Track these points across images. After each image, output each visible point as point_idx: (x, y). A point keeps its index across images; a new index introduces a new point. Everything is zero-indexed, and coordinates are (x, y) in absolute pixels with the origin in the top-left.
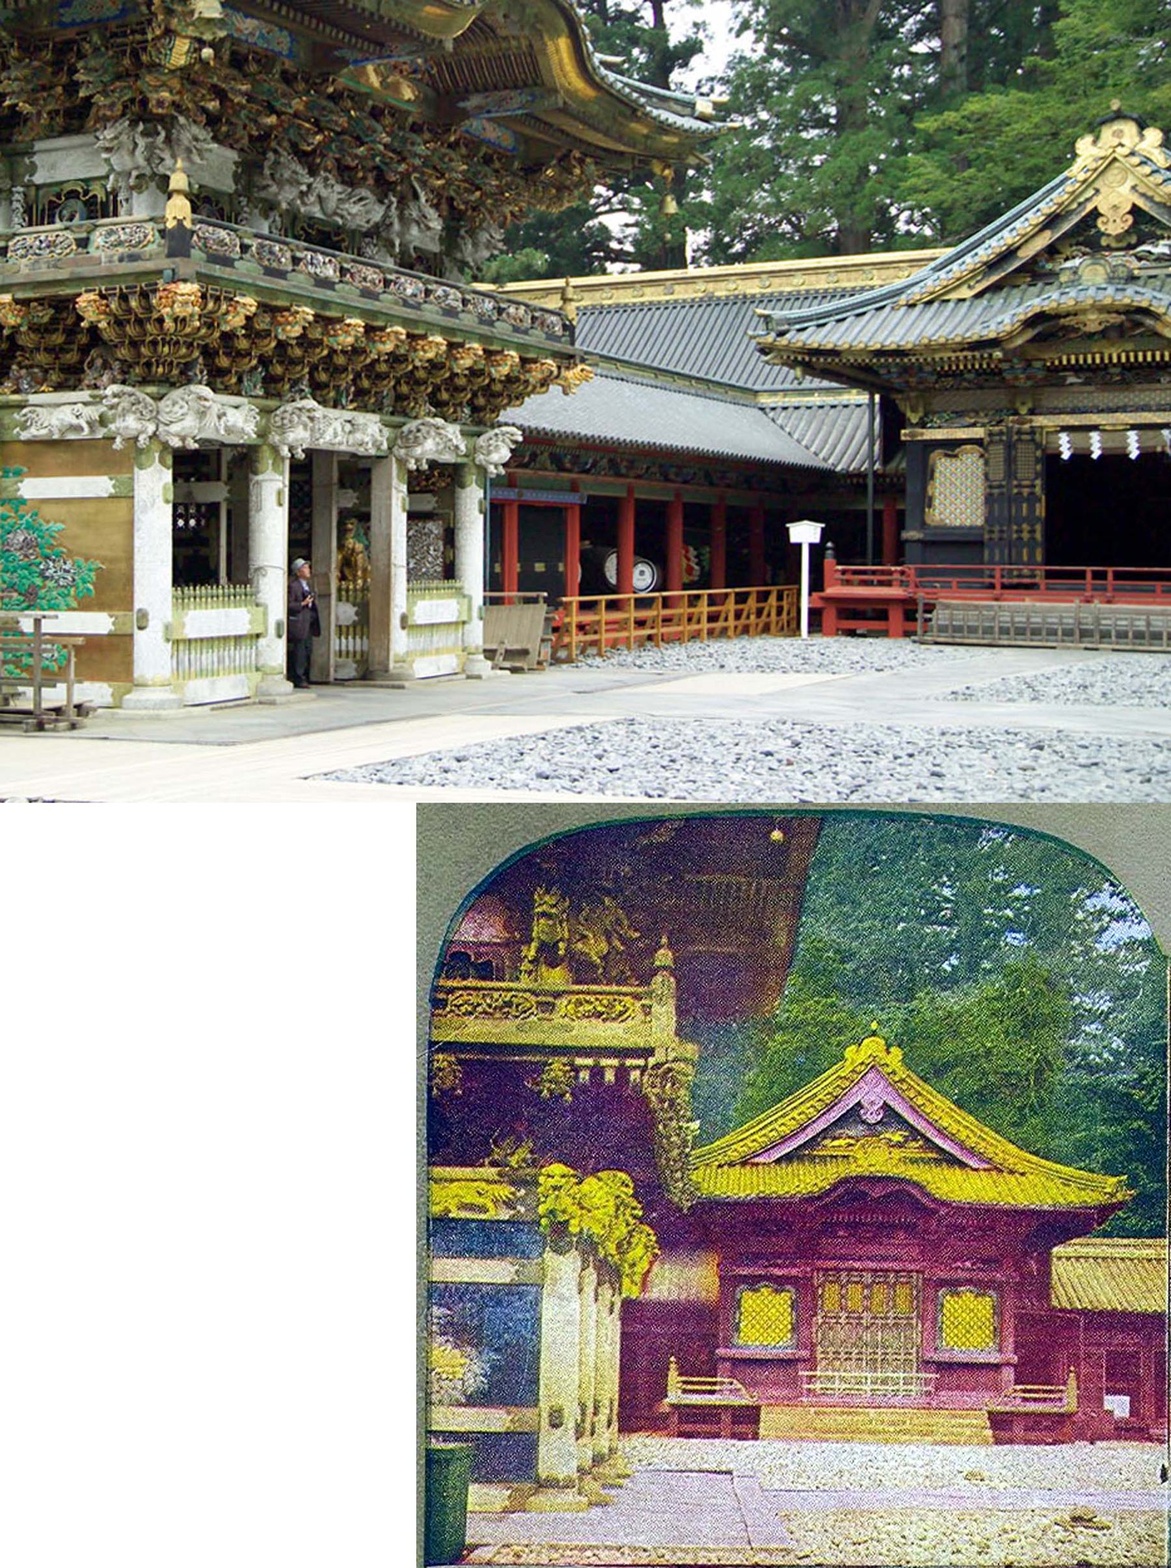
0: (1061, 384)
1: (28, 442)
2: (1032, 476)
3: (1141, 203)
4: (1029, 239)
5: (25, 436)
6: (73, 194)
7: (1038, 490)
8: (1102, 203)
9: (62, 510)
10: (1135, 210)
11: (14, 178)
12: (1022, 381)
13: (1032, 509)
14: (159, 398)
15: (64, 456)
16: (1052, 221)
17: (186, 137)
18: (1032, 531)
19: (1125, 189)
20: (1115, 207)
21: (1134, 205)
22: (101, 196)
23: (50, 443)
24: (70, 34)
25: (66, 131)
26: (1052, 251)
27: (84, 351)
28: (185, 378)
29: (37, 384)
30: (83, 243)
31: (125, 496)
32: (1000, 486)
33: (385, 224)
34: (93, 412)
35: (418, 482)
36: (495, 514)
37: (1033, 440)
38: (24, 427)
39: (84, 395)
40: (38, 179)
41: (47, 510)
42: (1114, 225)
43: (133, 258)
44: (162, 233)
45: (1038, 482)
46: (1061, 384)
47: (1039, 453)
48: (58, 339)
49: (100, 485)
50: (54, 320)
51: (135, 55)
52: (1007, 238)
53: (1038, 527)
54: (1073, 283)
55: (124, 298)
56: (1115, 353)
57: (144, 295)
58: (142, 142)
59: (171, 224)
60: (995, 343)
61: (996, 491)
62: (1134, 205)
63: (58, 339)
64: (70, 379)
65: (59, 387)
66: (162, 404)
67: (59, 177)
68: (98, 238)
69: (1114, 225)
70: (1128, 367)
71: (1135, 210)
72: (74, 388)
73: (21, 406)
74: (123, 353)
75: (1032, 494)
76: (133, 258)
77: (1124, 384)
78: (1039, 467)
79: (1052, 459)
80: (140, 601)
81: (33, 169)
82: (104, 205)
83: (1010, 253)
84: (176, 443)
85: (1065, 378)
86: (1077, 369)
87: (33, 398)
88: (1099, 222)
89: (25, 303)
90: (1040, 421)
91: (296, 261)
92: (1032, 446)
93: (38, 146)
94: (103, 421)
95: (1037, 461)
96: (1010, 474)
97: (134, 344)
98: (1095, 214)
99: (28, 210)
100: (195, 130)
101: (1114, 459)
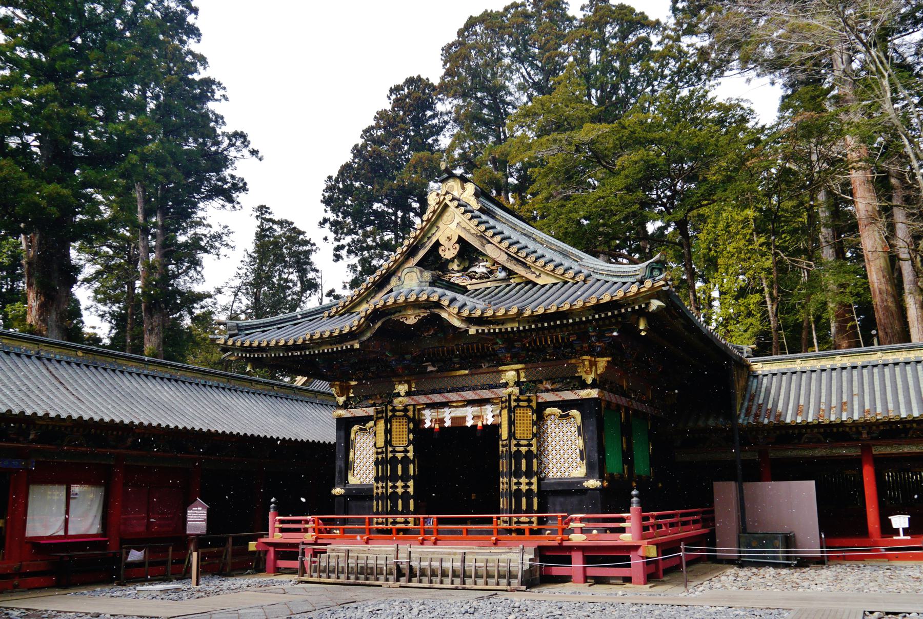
2: (405, 443)
3: (463, 236)
7: (411, 455)
10: (461, 240)
13: (405, 470)
18: (406, 487)
19: (453, 226)
20: (449, 239)
21: (460, 237)
32: (382, 453)
37: (406, 416)
45: (411, 448)
47: (411, 426)
53: (411, 483)
61: (380, 456)
62: (460, 237)
69: (449, 252)
71: (461, 240)
75: (406, 457)
78: (411, 436)
85: (426, 367)
88: (441, 249)
92: (405, 420)
95: (410, 431)
96: (388, 442)
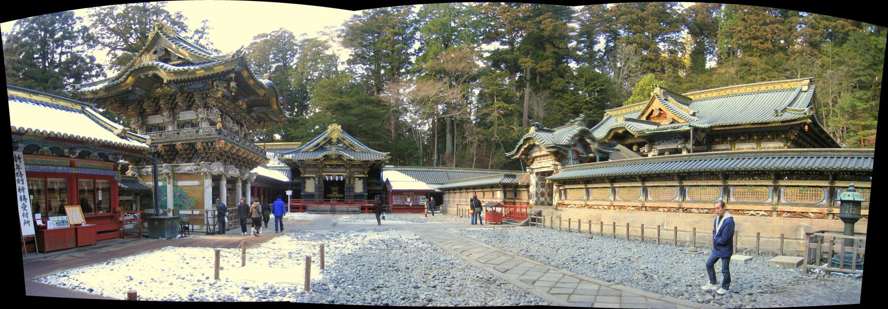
0: (326, 167)
1: (180, 174)
4: (322, 142)
5: (179, 172)
6: (188, 122)
8: (333, 137)
9: (187, 188)
11: (174, 119)
12: (320, 167)
14: (210, 164)
15: (188, 177)
16: (325, 139)
17: (215, 111)
22: (195, 123)
23: (185, 174)
24: (192, 90)
25: (187, 110)
26: (325, 144)
27: (193, 154)
28: (214, 162)
29: (182, 162)
30: (197, 132)
31: (202, 185)
33: (238, 131)
34: (195, 167)
35: (243, 181)
36: (252, 188)
38: (178, 171)
39: (193, 164)
40: (180, 119)
41: (184, 188)
42: (334, 141)
43: (209, 135)
44: (216, 130)
46: (326, 167)
48: (189, 152)
49: (196, 183)
50: (188, 148)
51: (206, 95)
52: (318, 141)
54: (331, 150)
55: (207, 143)
56: (334, 162)
57: (212, 143)
58: (206, 112)
59: (218, 128)
60: (318, 160)
63: (189, 152)
64: (189, 160)
65: (187, 162)
66: (211, 166)
67: (185, 119)
68: (201, 131)
69: (334, 141)
70: (336, 165)
72: (190, 162)
73: (178, 166)
74: (204, 155)
76: (209, 135)
77: (336, 168)
79: (325, 180)
80: (206, 207)
81: (179, 117)
82: (195, 125)
83: (318, 144)
84: (214, 174)
86: (329, 165)
87: (181, 164)
89: (183, 144)
90: (323, 174)
91: (234, 137)
93: (181, 113)
94: (197, 170)
96: (319, 183)
97: (207, 153)
98: (332, 138)
99: (178, 126)
100: (217, 110)
101: (334, 181)
